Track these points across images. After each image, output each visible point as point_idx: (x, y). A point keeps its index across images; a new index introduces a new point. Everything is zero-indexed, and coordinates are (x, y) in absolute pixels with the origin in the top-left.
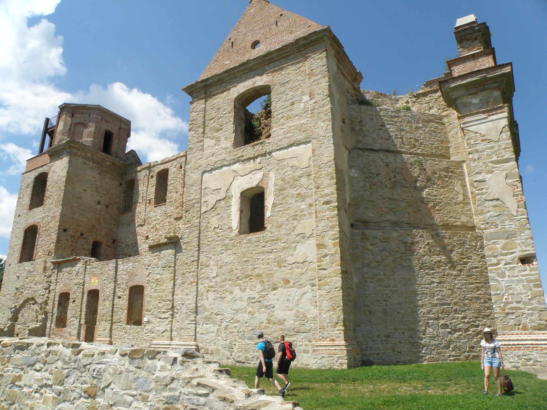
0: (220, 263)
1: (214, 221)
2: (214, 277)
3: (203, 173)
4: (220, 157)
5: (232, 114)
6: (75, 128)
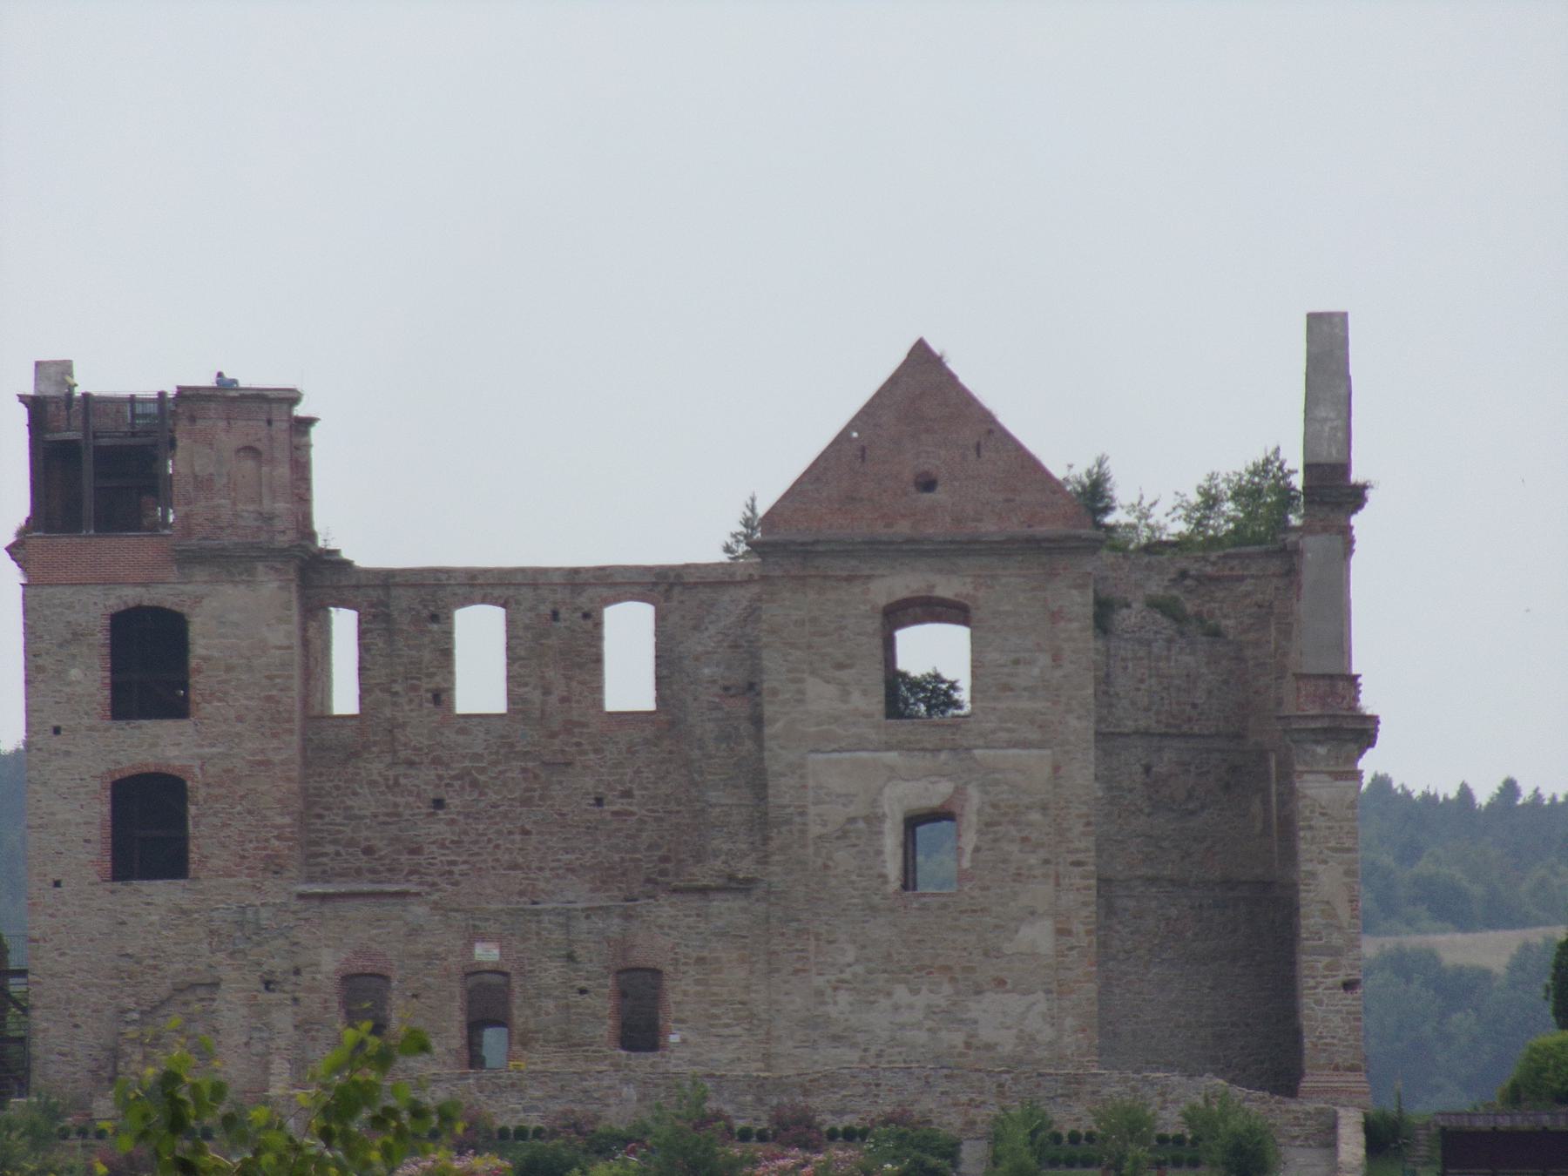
1: (843, 858)
2: (849, 965)
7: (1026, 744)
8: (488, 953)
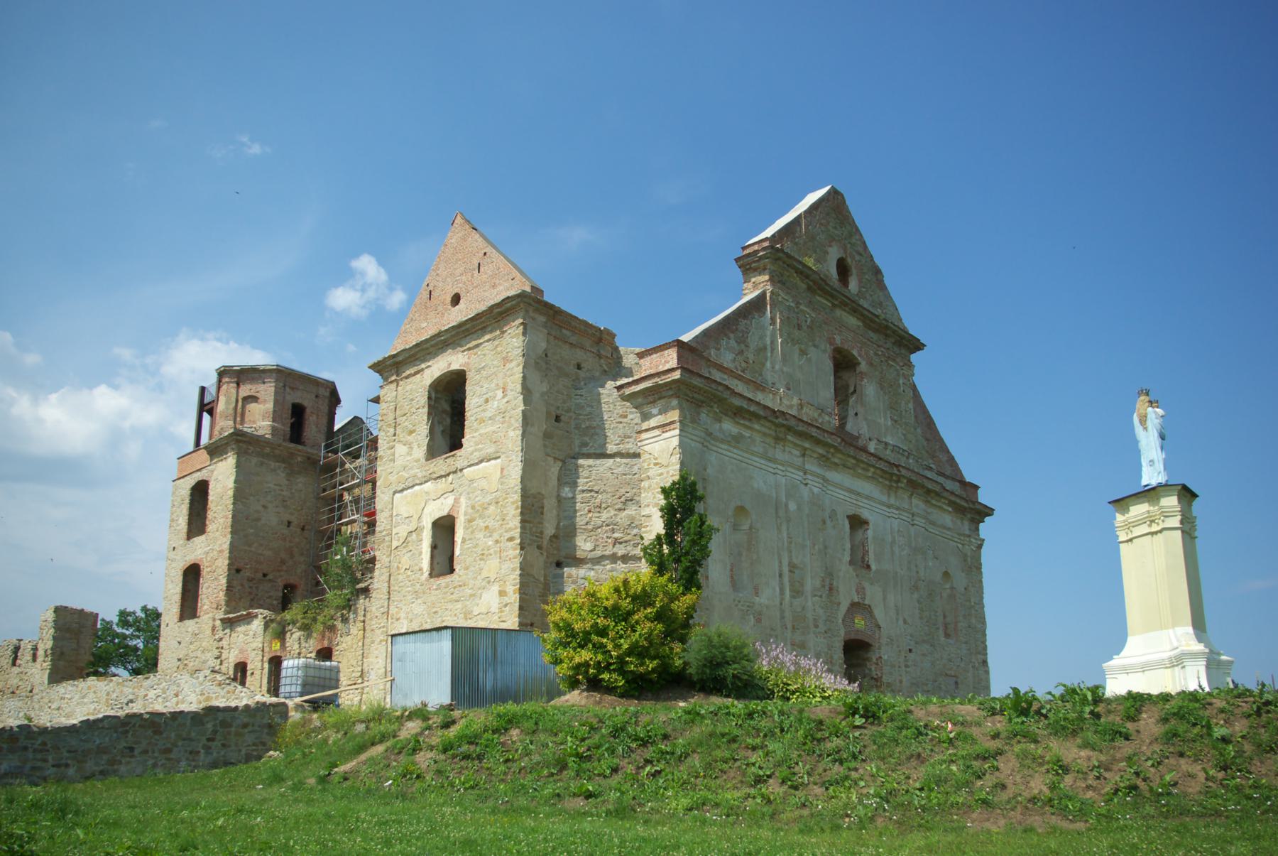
0: (410, 616)
3: (395, 493)
4: (412, 472)
5: (426, 410)
6: (243, 407)
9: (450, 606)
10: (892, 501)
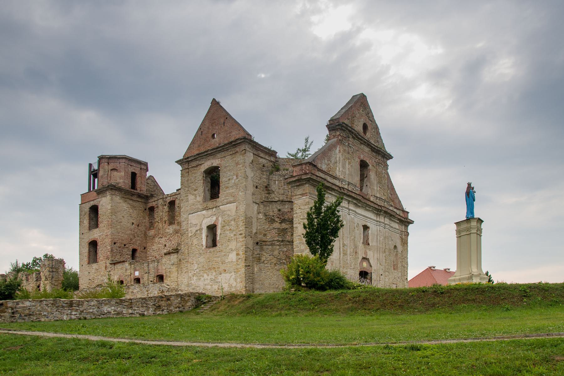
1: (195, 242)
5: (202, 181)
7: (230, 203)
8: (137, 274)
9: (215, 259)
10: (378, 220)
